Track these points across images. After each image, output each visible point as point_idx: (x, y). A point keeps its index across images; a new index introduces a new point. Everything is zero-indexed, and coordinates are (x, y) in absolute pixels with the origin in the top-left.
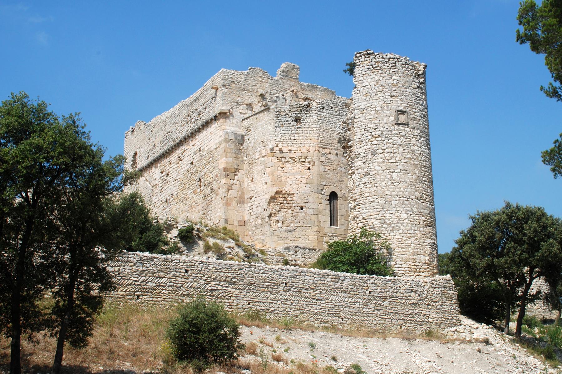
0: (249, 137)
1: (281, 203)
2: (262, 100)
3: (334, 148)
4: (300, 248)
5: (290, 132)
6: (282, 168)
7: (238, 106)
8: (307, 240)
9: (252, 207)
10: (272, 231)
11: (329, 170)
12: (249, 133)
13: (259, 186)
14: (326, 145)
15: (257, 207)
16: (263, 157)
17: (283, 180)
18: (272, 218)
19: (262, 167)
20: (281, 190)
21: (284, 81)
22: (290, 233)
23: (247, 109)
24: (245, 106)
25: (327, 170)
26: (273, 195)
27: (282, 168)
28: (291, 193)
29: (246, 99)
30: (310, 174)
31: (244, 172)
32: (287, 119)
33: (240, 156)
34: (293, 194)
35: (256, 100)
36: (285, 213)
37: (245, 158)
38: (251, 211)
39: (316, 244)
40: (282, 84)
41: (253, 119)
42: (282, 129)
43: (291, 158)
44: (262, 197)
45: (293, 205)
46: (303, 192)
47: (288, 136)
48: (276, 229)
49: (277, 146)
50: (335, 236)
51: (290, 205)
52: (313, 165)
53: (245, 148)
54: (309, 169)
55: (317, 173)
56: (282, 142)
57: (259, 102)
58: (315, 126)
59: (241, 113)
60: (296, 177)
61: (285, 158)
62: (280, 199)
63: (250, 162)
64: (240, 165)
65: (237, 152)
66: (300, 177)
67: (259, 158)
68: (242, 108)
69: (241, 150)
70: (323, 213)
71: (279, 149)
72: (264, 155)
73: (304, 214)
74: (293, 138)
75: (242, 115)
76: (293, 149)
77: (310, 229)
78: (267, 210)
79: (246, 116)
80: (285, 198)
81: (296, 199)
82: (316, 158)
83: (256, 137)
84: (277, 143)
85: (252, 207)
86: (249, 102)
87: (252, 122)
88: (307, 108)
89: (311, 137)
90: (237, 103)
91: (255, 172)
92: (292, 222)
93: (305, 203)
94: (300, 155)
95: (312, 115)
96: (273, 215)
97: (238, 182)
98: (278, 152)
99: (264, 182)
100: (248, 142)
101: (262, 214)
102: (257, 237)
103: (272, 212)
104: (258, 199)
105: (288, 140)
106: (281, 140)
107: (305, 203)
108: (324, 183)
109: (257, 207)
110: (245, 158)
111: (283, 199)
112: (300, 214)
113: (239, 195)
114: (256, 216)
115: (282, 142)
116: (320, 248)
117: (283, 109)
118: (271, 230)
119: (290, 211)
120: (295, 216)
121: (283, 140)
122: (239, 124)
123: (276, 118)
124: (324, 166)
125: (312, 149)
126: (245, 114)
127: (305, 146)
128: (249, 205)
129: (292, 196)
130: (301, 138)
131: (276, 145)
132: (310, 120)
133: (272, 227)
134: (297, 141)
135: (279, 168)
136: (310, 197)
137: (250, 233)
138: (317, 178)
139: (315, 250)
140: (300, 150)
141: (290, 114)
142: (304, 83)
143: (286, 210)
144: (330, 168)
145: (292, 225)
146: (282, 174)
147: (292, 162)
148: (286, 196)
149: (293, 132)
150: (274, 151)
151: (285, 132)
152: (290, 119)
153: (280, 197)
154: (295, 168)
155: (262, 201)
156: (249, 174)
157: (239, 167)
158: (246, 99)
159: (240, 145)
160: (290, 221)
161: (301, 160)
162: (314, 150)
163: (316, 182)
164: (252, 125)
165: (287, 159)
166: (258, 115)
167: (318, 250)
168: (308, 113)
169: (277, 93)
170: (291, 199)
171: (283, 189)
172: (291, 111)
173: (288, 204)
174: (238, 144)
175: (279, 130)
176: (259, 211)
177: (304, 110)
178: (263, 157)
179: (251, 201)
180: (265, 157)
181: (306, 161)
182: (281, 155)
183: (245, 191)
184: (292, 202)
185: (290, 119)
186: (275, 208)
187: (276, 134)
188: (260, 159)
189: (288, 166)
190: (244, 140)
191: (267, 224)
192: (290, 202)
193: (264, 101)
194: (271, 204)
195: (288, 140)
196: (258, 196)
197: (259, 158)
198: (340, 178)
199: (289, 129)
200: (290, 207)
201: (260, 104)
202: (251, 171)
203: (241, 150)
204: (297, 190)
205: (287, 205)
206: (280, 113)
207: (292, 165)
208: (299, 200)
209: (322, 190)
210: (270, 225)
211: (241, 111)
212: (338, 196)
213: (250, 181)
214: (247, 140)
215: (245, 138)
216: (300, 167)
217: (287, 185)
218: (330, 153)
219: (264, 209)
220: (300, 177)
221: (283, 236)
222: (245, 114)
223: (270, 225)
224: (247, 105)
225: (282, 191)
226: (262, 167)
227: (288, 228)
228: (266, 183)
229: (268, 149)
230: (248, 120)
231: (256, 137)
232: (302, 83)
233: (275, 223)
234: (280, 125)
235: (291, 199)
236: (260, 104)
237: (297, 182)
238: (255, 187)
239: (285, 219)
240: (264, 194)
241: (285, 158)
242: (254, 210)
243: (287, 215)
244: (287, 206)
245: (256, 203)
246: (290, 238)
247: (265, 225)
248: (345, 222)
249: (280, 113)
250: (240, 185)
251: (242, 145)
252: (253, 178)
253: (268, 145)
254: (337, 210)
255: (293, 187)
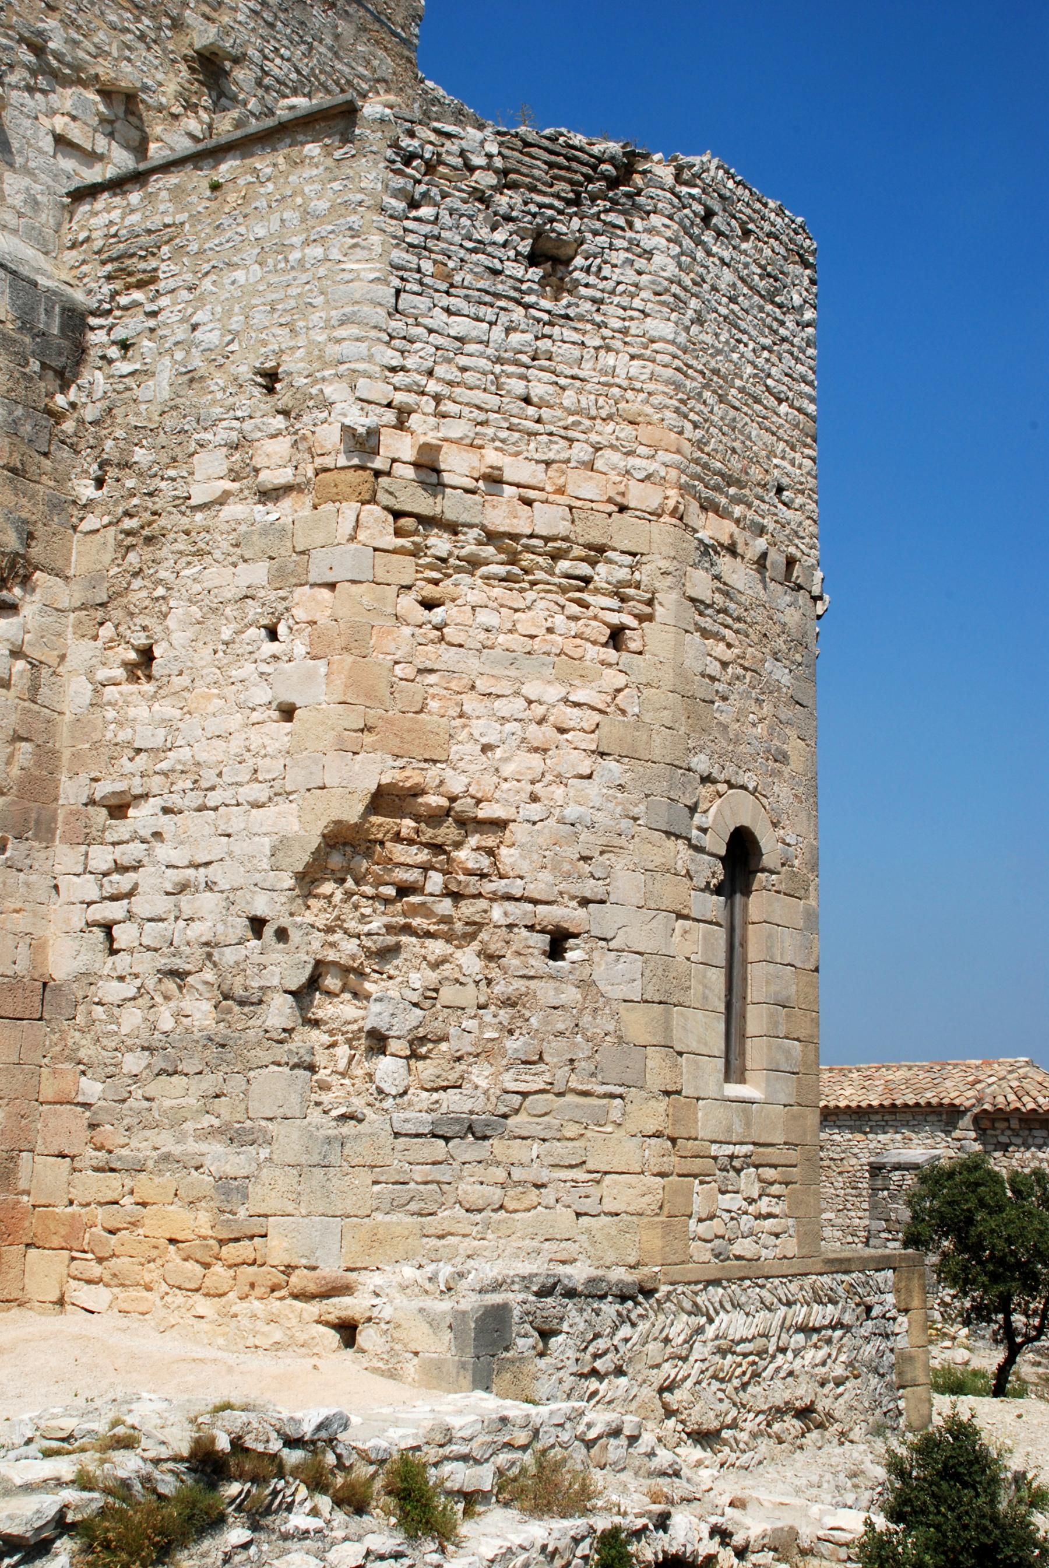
0: (129, 327)
1: (404, 890)
2: (206, 101)
3: (750, 514)
4: (571, 1293)
5: (498, 333)
6: (429, 605)
7: (42, 82)
8: (586, 1206)
9: (123, 882)
10: (331, 1129)
11: (725, 665)
12: (137, 295)
13: (214, 726)
14: (717, 488)
15: (183, 888)
16: (268, 495)
17: (433, 705)
18: (324, 1008)
19: (257, 573)
20: (412, 777)
21: (342, 26)
22: (466, 1149)
23: (108, 126)
24: (93, 96)
25: (714, 669)
26: (352, 812)
27: (429, 605)
28: (485, 812)
29: (101, 52)
30: (621, 680)
31: (66, 595)
32: (483, 233)
33: (47, 464)
34: (499, 825)
35: (171, 88)
36: (432, 977)
37: (86, 490)
38: (114, 911)
39: (652, 1240)
40: (329, 41)
41: (177, 194)
42: (446, 301)
43: (491, 537)
44: (235, 819)
45: (497, 913)
46: (572, 812)
47: (483, 363)
48: (358, 1104)
49: (400, 425)
50: (749, 1161)
51: (469, 909)
52: (641, 618)
53: (90, 413)
54: (616, 637)
55: (667, 677)
56: (437, 398)
57: (191, 107)
58: (667, 330)
59: (61, 141)
60: (530, 690)
61: (453, 528)
62: (400, 852)
63: (128, 524)
64: (40, 531)
65: (27, 429)
66: (553, 693)
67: (222, 500)
68: (68, 106)
69: (57, 416)
70: (693, 996)
71: (426, 448)
72: (270, 478)
73: (571, 995)
74: (518, 387)
75: (67, 164)
76: (515, 470)
77: (615, 1115)
78: (282, 935)
79: (94, 175)
80: (437, 848)
81: (524, 867)
82: (665, 564)
83: (209, 336)
84: (400, 397)
85: (123, 882)
86: (128, 76)
87: (164, 211)
88: (613, 183)
89: (635, 404)
90: (38, 50)
91: (180, 610)
92: (484, 1053)
93: (585, 902)
94: (563, 528)
95: (648, 242)
96: (331, 982)
97: (20, 665)
98: (409, 472)
99: (261, 694)
100: (124, 367)
101: (229, 956)
102: (166, 1142)
103: (331, 955)
104: (192, 822)
105: (478, 396)
106: (432, 387)
107: (585, 902)
108: (701, 763)
109: (183, 888)
110: (86, 490)
111: (423, 856)
112: (546, 992)
113: (15, 771)
114: (163, 962)
115: (437, 398)
116: (676, 1272)
117: (452, 146)
118: (315, 1116)
119: (468, 959)
120: (509, 1003)
121: (445, 390)
122: (47, 218)
123: (400, 205)
124: (705, 633)
125: (640, 496)
126: (92, 157)
127: (590, 466)
128: (102, 857)
129: (490, 841)
130: (569, 398)
131: (390, 416)
132: (630, 276)
133: (324, 1087)
134: (545, 413)
135: (408, 603)
136: (619, 863)
137: (91, 1088)
138: (666, 716)
139: (649, 1293)
140: (561, 491)
141: (503, 201)
142: (441, 92)
143: (437, 948)
144: (728, 655)
145: (480, 1075)
146: (428, 655)
147: (501, 570)
148: (448, 832)
149: (515, 338)
150: (379, 463)
151: (460, 326)
152: (499, 236)
153: (398, 838)
154: (526, 622)
155: (239, 847)
156: (117, 614)
157: (36, 551)
158: (101, 52)
159: (51, 382)
160: (466, 1045)
161: (564, 565)
162: (654, 504)
163: (660, 746)
164: (168, 233)
165: (469, 543)
166: (227, 168)
167: (664, 1289)
168: (621, 221)
169: (295, 92)
170: (485, 862)
171: (433, 773)
172: (507, 181)
173: (456, 897)
174: (35, 365)
175: (423, 303)
176: (199, 931)
177: (593, 199)
178: (268, 495)
179: (121, 829)
180: (287, 503)
181: (599, 582)
182: (422, 503)
183: (64, 741)
184: (487, 887)
185: (499, 236)
186: (352, 925)
187: (396, 325)
188: (232, 510)
189: (474, 597)
190: (80, 352)
191: (280, 1052)
192: (473, 884)
193: (217, 107)
194: (327, 888)
195: (478, 396)
196: (194, 799)
197: (222, 500)
198: (771, 729)
199: (489, 313)
200: (476, 927)
201: (192, 124)
202: (139, 592)
203: (57, 416)
204: (534, 798)
205: (445, 906)
206: (430, 168)
207: (498, 591)
208: (546, 876)
209: (693, 809)
210: (312, 1068)
211: (60, 123)
212: (767, 861)
213: (120, 673)
214: (114, 352)
215: (96, 337)
216: (559, 620)
217: (464, 749)
218: (732, 550)
219: (257, 925)
220: (553, 693)
221: (420, 1172)
222: (92, 157)
223: (312, 1068)
224: (106, 94)
225: (417, 792)
226: (257, 573)
227: (450, 1100)
228: (288, 712)
229: (330, 436)
230: (135, 197)
231: (209, 336)
232: (430, 84)
233: (343, 1052)
234: (427, 266)
235: (485, 862)
236: (192, 124)
237: (537, 734)
238: (167, 723)
239: (436, 1027)
240: (258, 792)
241: (453, 528)
242: (141, 906)
243: (448, 994)
244: (446, 920)
245: (163, 852)
246: (470, 1190)
247: (262, 1055)
248: (787, 1052)
249: (430, 168)
250: (35, 688)
251: (65, 379)
252: (147, 655)
253: (328, 405)
254: (745, 962)
255: (507, 770)
